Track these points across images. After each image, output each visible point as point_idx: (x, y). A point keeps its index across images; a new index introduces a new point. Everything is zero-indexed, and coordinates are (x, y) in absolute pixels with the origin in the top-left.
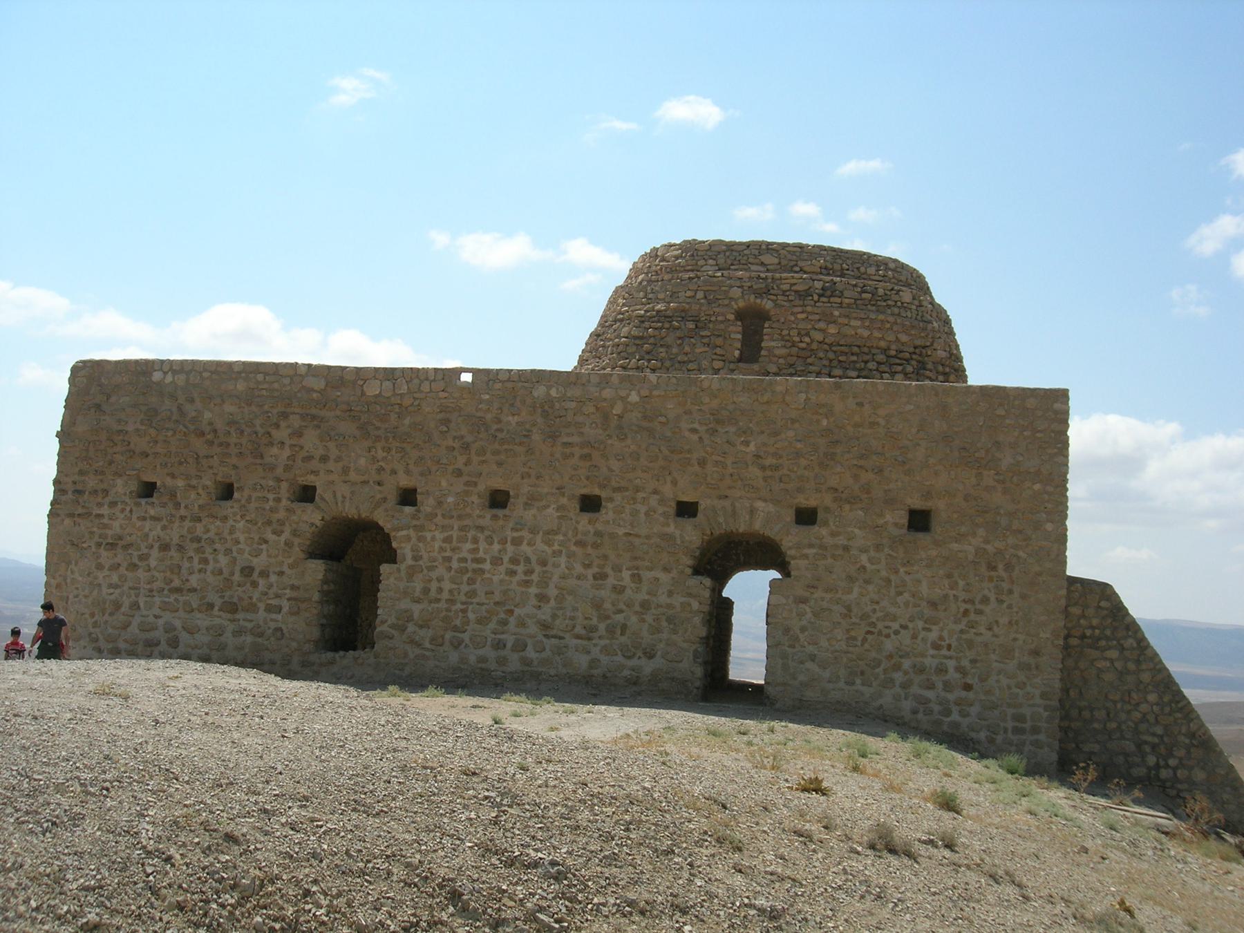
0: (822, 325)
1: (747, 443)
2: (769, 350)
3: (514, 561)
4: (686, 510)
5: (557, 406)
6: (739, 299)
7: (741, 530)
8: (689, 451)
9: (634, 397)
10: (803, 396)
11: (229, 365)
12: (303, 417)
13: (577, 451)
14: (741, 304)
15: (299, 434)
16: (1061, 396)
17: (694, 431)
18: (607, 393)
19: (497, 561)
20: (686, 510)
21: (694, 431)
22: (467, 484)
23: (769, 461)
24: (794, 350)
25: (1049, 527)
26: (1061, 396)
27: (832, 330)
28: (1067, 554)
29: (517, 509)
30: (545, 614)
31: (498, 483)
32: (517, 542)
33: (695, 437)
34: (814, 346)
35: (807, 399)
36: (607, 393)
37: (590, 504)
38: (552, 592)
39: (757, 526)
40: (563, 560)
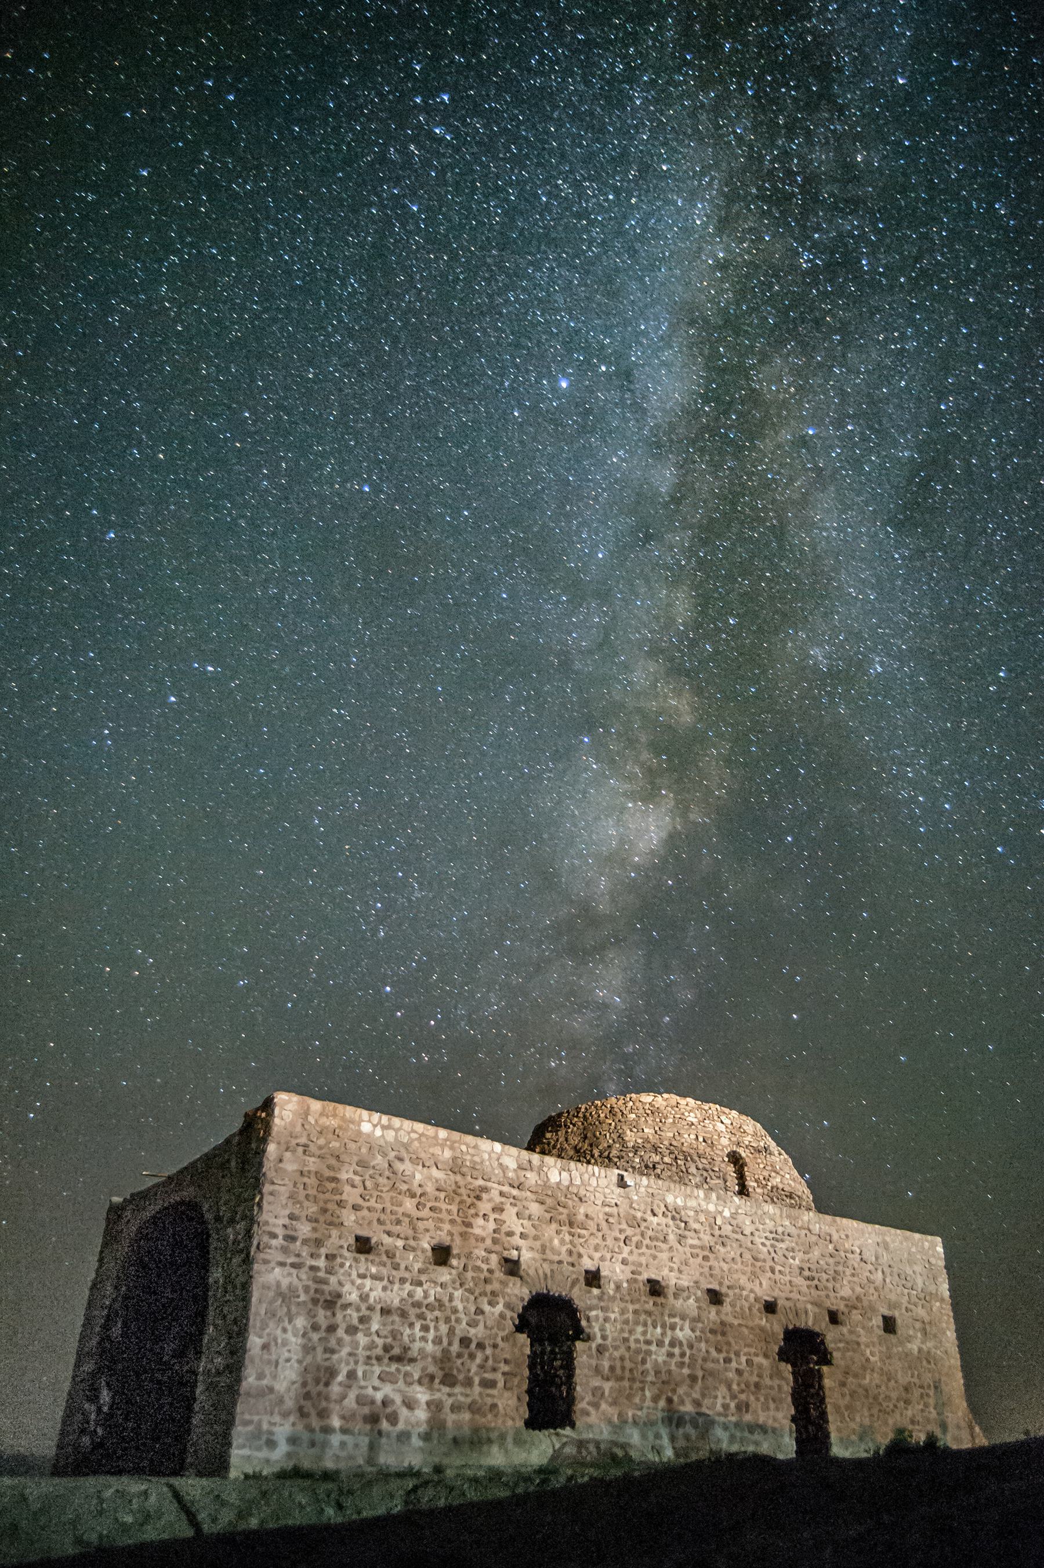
9: (727, 1213)
17: (763, 1244)
33: (765, 1250)
38: (700, 1374)
40: (703, 1345)
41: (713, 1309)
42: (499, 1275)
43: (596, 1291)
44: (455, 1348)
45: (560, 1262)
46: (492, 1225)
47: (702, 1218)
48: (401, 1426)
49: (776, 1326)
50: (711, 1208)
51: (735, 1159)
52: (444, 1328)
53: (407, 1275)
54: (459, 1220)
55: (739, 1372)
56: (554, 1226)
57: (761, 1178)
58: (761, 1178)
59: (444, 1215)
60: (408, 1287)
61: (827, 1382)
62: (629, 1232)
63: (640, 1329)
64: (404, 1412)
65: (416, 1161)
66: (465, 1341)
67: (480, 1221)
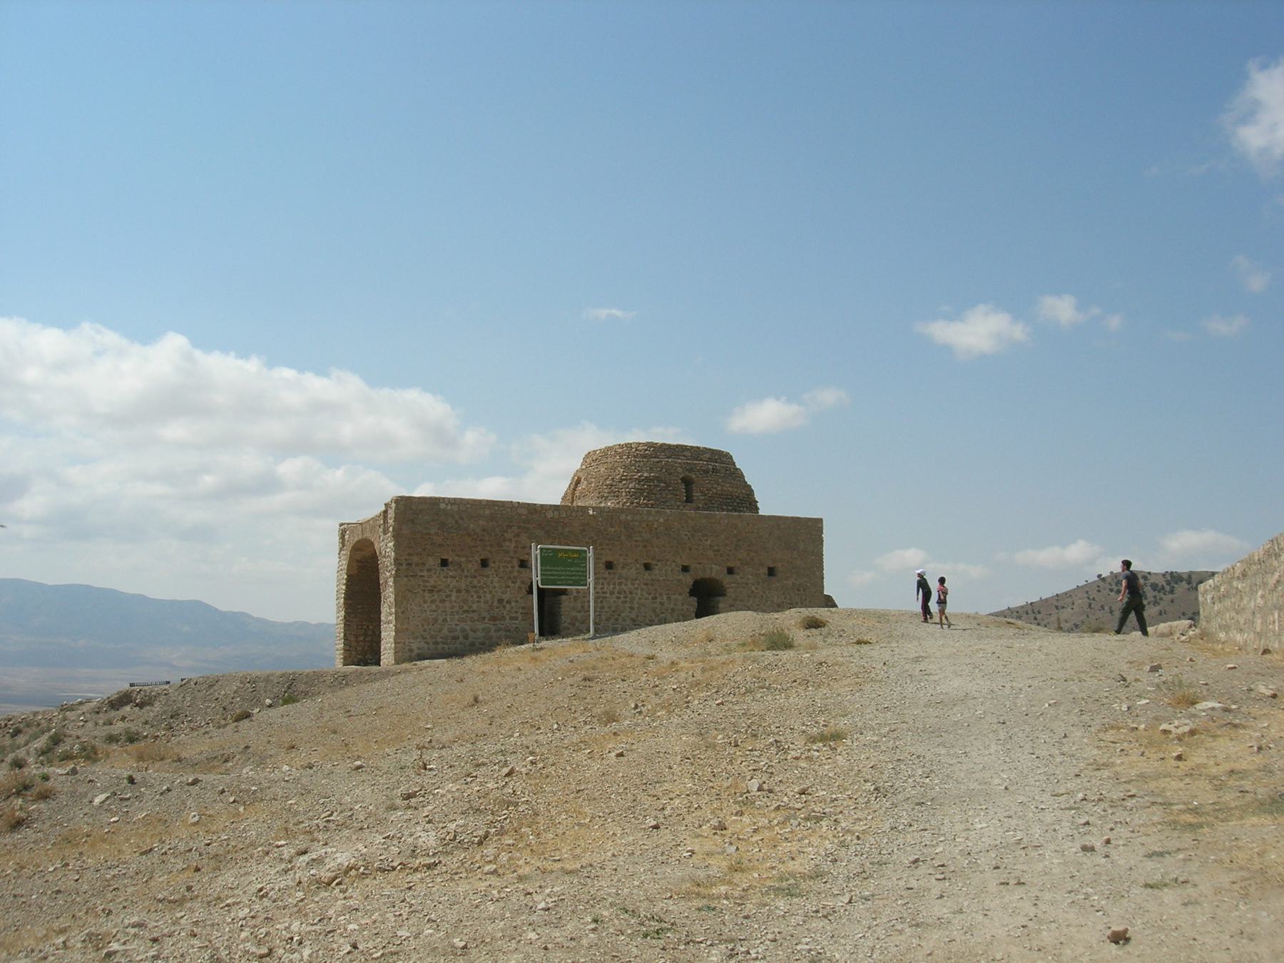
4: (685, 569)
9: (661, 520)
11: (480, 501)
12: (519, 527)
15: (518, 535)
16: (820, 520)
18: (651, 518)
19: (612, 593)
20: (685, 569)
26: (820, 520)
28: (223, 606)
30: (633, 615)
31: (610, 559)
32: (620, 584)
36: (651, 518)
37: (647, 567)
38: (636, 606)
40: (639, 592)
41: (647, 573)
42: (517, 568)
44: (495, 604)
46: (513, 545)
48: (470, 639)
49: (688, 580)
52: (489, 597)
55: (662, 604)
60: (469, 579)
64: (471, 634)
66: (500, 601)
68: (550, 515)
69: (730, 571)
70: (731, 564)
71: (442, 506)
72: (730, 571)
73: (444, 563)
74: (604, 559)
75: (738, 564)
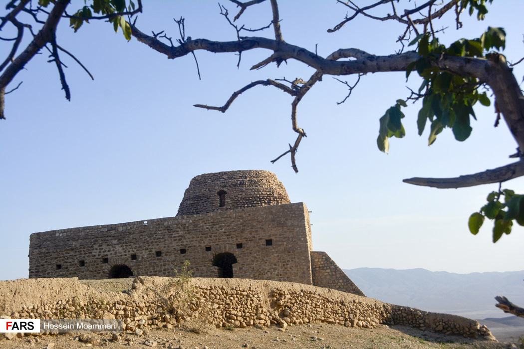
0: (240, 193)
1: (222, 229)
2: (228, 202)
3: (165, 270)
4: (208, 249)
5: (171, 227)
6: (218, 189)
7: (223, 252)
8: (207, 234)
9: (191, 221)
10: (235, 214)
13: (178, 238)
14: (218, 190)
16: (301, 204)
17: (207, 228)
20: (208, 249)
21: (207, 228)
22: (149, 252)
23: (227, 233)
24: (234, 201)
25: (302, 239)
26: (301, 204)
27: (244, 194)
29: (164, 257)
33: (208, 230)
34: (239, 199)
35: (236, 215)
39: (227, 250)
43: (134, 261)
45: (122, 255)
47: (180, 226)
49: (210, 255)
50: (184, 221)
51: (222, 194)
53: (71, 272)
54: (86, 252)
56: (120, 245)
57: (233, 196)
58: (233, 196)
59: (83, 252)
61: (234, 269)
62: (148, 239)
63: (151, 268)
65: (73, 239)
67: (95, 251)
68: (121, 229)
69: (239, 246)
70: (240, 241)
71: (57, 235)
72: (239, 246)
73: (59, 267)
74: (154, 251)
75: (244, 241)
